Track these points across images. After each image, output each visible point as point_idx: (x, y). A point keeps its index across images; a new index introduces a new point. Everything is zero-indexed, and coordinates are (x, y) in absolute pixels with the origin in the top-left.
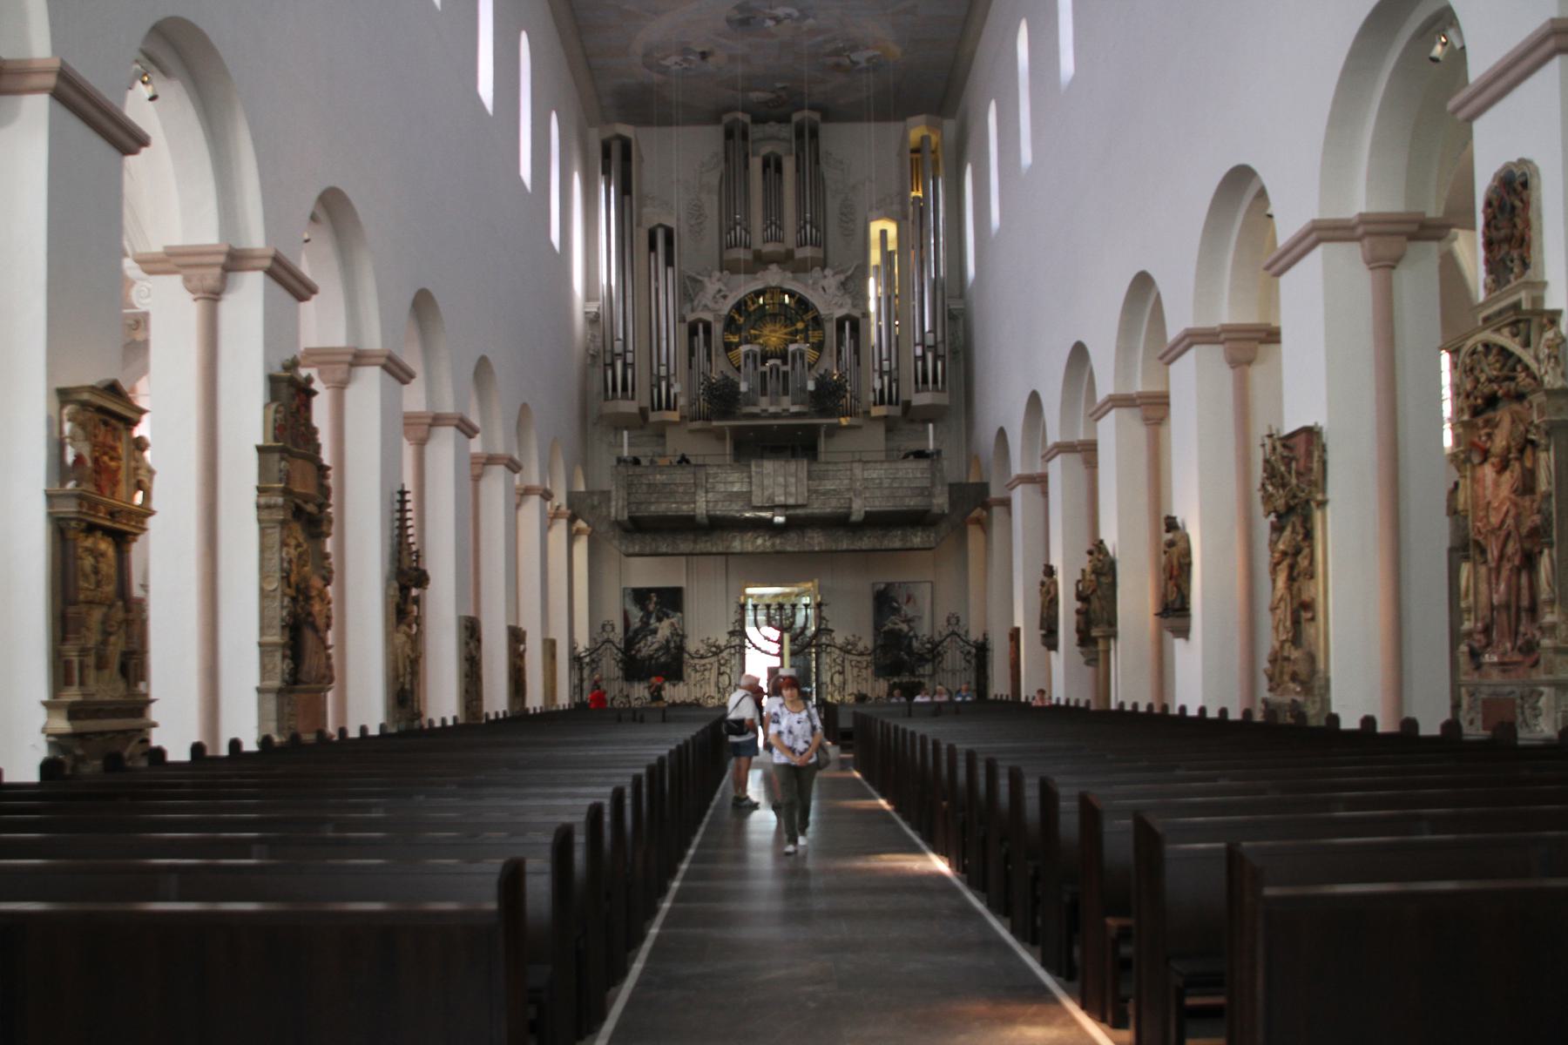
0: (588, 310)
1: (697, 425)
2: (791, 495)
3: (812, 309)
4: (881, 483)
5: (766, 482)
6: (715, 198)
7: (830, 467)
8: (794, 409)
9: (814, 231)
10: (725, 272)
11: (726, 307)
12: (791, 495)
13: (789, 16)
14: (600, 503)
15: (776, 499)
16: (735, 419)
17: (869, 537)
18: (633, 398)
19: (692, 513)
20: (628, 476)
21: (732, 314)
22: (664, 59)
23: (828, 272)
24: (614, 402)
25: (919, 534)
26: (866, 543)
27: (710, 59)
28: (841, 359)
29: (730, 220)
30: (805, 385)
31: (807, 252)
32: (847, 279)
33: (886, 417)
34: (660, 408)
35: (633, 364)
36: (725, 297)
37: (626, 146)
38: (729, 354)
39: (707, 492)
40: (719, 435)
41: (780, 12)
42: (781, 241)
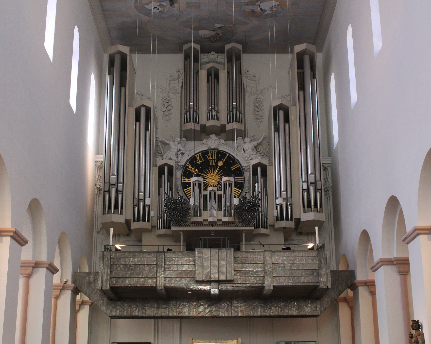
0: (97, 160)
1: (163, 231)
2: (223, 273)
4: (284, 267)
5: (205, 264)
8: (225, 219)
10: (183, 139)
11: (183, 161)
12: (223, 273)
15: (212, 276)
17: (276, 307)
18: (121, 213)
19: (154, 286)
20: (111, 258)
21: (187, 165)
23: (246, 139)
24: (109, 215)
25: (309, 305)
26: (273, 311)
28: (255, 191)
29: (187, 106)
31: (235, 126)
32: (259, 144)
33: (285, 228)
34: (139, 220)
35: (122, 191)
36: (183, 154)
37: (124, 59)
38: (185, 190)
39: (165, 271)
40: (175, 237)
42: (218, 119)
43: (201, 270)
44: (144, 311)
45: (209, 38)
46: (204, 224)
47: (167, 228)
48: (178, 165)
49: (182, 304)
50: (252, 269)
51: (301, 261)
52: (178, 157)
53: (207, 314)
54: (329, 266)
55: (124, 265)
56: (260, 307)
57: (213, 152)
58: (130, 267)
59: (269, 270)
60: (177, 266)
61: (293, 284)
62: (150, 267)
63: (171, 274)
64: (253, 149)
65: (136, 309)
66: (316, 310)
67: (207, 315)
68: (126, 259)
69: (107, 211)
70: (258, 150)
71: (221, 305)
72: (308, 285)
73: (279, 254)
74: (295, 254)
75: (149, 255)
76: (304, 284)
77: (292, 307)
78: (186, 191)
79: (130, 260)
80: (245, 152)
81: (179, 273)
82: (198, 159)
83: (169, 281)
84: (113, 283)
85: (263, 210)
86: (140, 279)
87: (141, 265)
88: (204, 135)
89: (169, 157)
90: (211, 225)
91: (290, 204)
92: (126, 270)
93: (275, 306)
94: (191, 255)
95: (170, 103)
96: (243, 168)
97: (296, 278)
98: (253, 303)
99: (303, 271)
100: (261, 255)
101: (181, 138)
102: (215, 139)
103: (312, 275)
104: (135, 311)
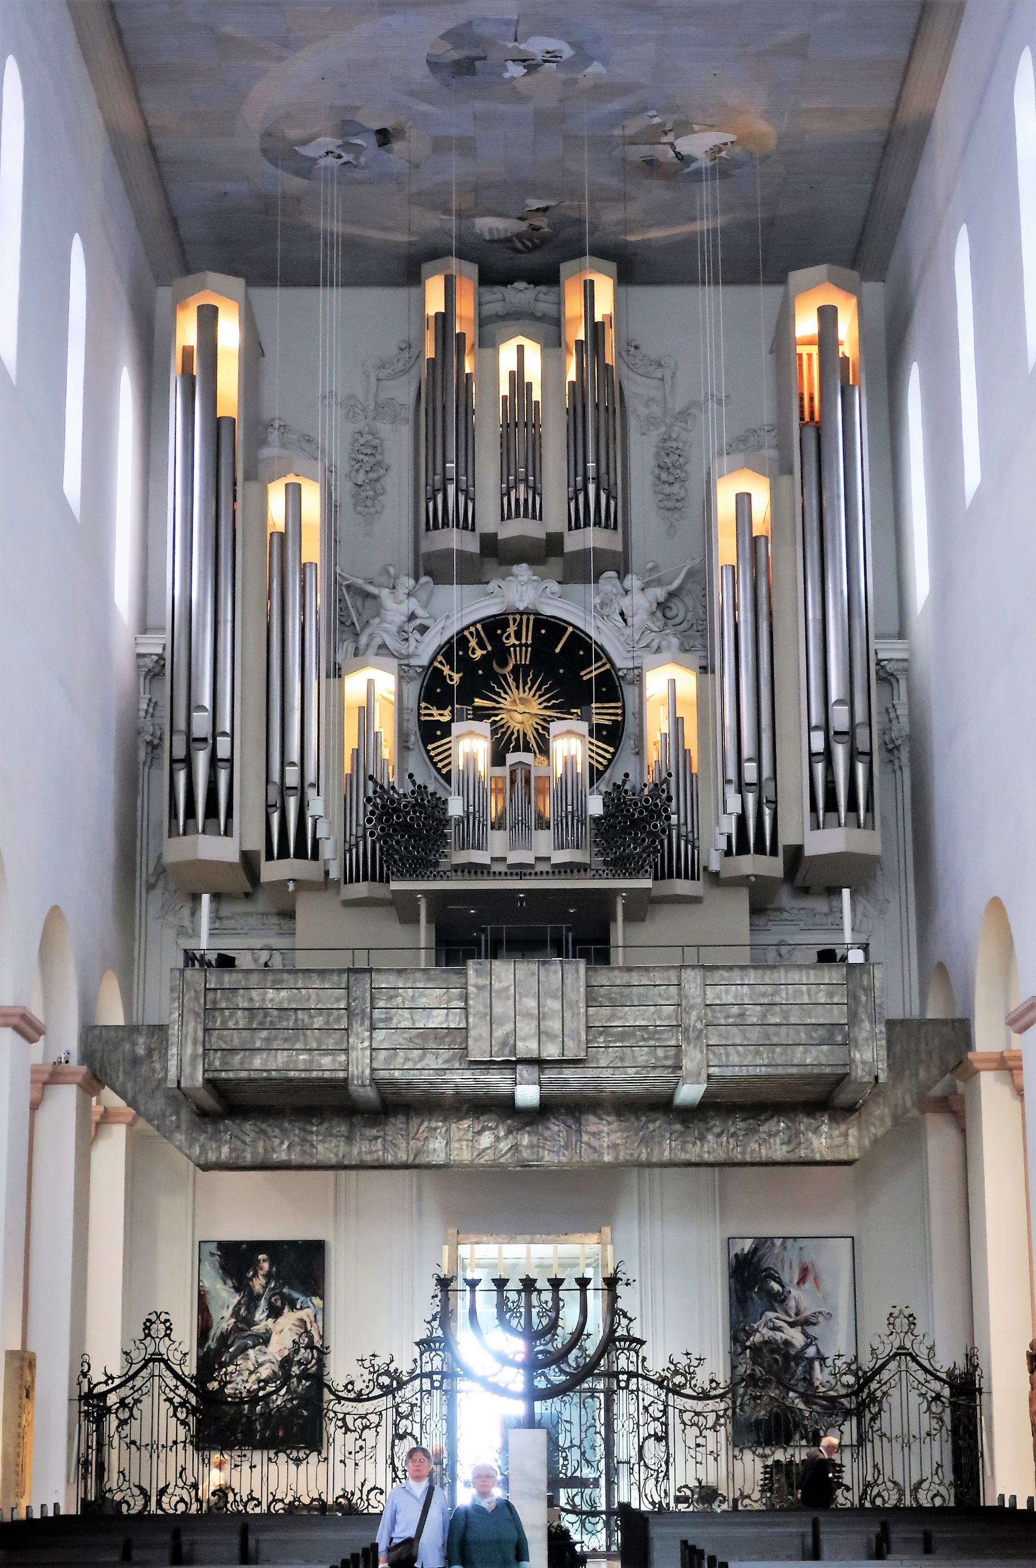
1: (361, 889)
2: (551, 1037)
3: (598, 658)
4: (742, 1015)
5: (498, 1009)
6: (406, 431)
7: (635, 978)
8: (561, 857)
9: (603, 497)
10: (424, 579)
12: (551, 1037)
13: (552, 57)
14: (150, 1052)
15: (520, 1045)
16: (442, 876)
17: (719, 1135)
18: (228, 832)
19: (341, 1075)
21: (436, 664)
22: (305, 142)
23: (633, 581)
25: (825, 1128)
27: (397, 146)
29: (435, 474)
30: (584, 807)
31: (592, 538)
32: (671, 595)
34: (284, 854)
35: (230, 761)
36: (423, 629)
38: (430, 747)
39: (373, 1028)
41: (536, 46)
42: (537, 515)
43: (484, 1028)
44: (307, 1147)
45: (509, 240)
46: (492, 870)
47: (374, 879)
48: (408, 665)
49: (426, 1124)
50: (643, 1023)
51: (795, 997)
52: (407, 640)
53: (503, 1156)
54: (880, 1014)
55: (246, 1012)
56: (671, 1134)
57: (521, 619)
58: (265, 1017)
59: (694, 1026)
60: (410, 1013)
61: (770, 1070)
62: (329, 1015)
63: (394, 1037)
64: (653, 614)
65: (282, 1143)
66: (846, 1143)
67: (503, 1160)
68: (254, 994)
69: (181, 823)
70: (669, 614)
71: (548, 1129)
72: (816, 1071)
73: (725, 974)
74: (776, 975)
75: (323, 981)
76: (802, 1070)
77: (770, 1135)
78: (434, 749)
79: (265, 994)
80: (625, 621)
81: (418, 1035)
82: (473, 643)
83: (387, 1060)
84: (213, 1068)
85: (682, 821)
86: (297, 1055)
87: (299, 1012)
88: (490, 564)
89: (378, 641)
90: (517, 874)
91: (768, 801)
92: (254, 1026)
93: (717, 1130)
94: (455, 980)
95: (379, 458)
96: (620, 673)
97: (778, 1049)
98: (648, 1122)
99: (801, 1028)
100: (669, 979)
101: (417, 579)
102: (529, 580)
103: (829, 1041)
104: (277, 1149)
